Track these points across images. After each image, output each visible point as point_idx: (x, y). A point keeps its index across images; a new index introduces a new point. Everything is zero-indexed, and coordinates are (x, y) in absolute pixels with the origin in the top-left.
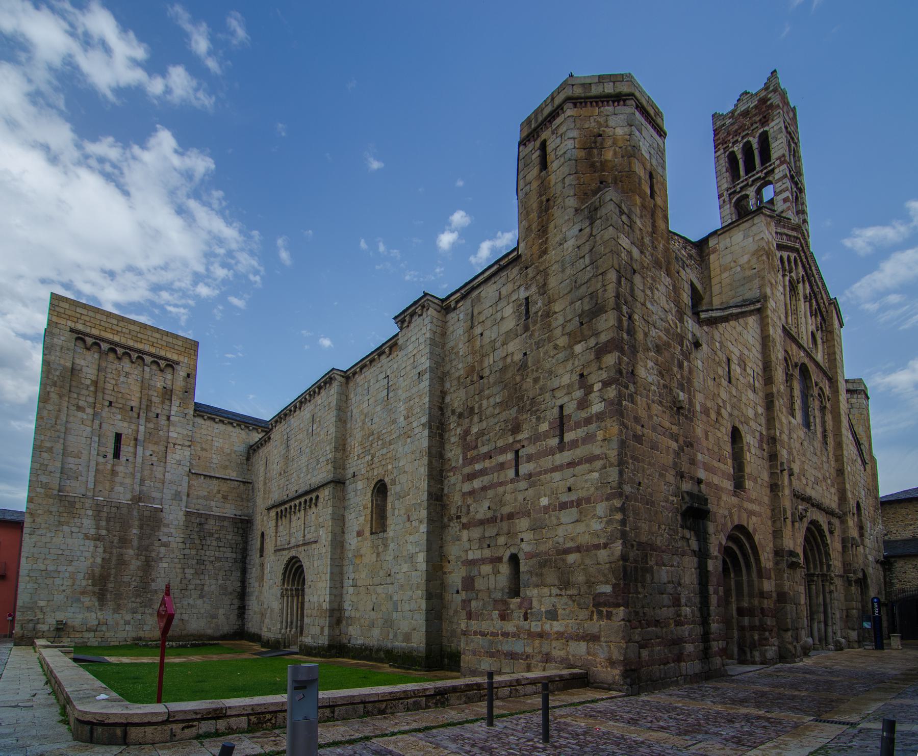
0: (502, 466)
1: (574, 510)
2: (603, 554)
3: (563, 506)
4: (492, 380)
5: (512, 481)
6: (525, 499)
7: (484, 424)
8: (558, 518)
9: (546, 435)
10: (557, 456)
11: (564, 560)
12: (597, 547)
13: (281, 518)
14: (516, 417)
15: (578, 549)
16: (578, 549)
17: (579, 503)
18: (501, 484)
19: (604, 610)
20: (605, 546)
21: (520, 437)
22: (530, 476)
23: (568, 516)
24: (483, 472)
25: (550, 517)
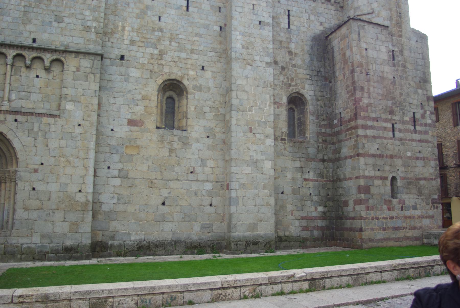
0: (385, 128)
1: (422, 161)
2: (434, 183)
3: (417, 158)
4: (375, 79)
5: (391, 139)
6: (399, 150)
7: (372, 101)
8: (416, 164)
9: (408, 123)
10: (414, 135)
11: (419, 183)
12: (432, 179)
14: (392, 107)
15: (425, 179)
16: (425, 179)
17: (424, 159)
18: (385, 138)
19: (435, 205)
20: (435, 180)
21: (394, 118)
22: (401, 139)
23: (420, 163)
24: (372, 127)
25: (412, 162)
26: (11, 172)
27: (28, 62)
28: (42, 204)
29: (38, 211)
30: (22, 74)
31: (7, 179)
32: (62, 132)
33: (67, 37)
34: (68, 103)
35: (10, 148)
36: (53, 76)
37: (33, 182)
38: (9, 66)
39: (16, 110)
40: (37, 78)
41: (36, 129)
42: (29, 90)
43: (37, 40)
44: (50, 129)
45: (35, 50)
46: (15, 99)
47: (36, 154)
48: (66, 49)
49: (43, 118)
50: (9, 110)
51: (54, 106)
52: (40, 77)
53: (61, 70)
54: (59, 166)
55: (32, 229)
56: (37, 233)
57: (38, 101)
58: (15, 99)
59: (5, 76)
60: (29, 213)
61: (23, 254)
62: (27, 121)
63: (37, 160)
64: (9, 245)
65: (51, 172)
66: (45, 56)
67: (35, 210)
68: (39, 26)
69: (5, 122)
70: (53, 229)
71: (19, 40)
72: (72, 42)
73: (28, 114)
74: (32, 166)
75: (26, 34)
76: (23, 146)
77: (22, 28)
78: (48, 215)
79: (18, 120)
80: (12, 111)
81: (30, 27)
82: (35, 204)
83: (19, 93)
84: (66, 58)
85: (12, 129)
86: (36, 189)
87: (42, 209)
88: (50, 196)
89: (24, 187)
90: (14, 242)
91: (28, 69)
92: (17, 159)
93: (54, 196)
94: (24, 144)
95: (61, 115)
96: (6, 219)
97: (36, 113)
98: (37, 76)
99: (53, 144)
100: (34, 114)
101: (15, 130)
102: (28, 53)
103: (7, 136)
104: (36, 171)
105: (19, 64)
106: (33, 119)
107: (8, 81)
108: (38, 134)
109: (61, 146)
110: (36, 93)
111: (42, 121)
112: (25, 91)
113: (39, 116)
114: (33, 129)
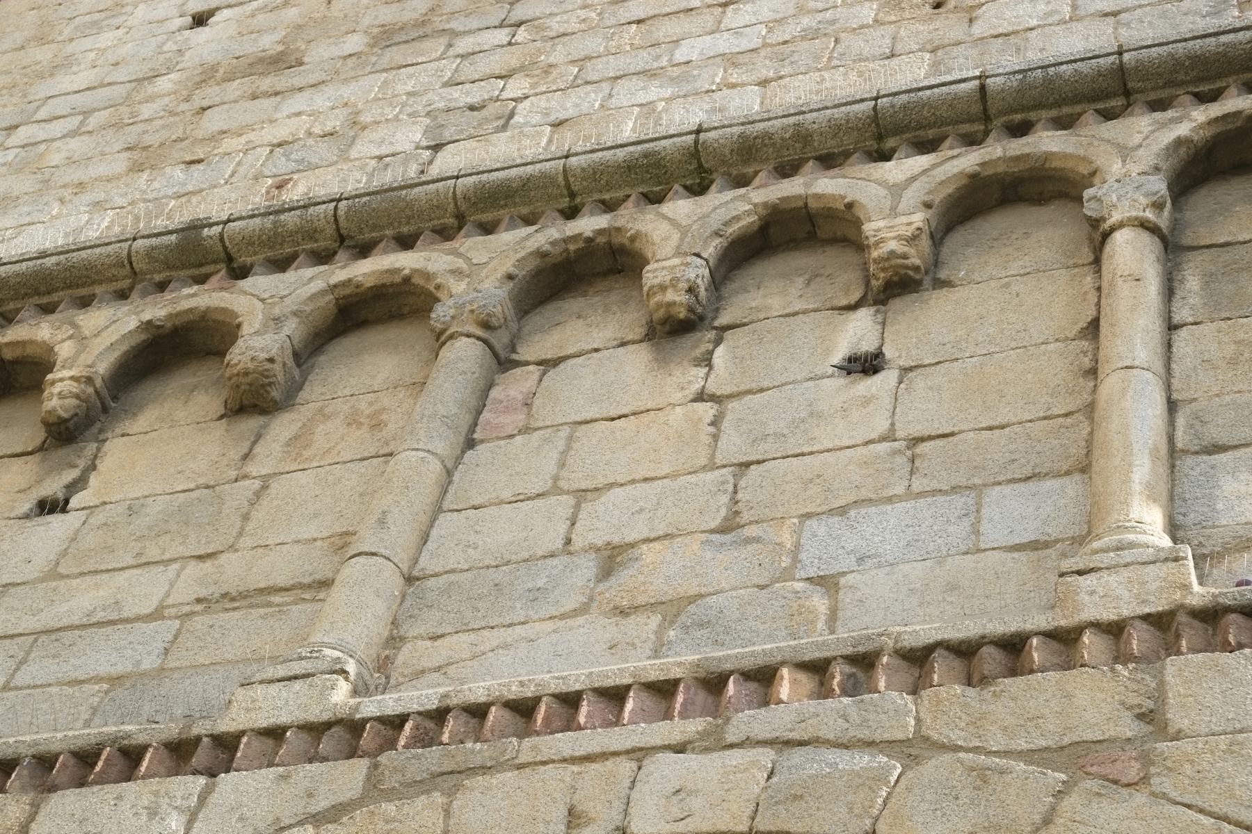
69: (1146, 760)
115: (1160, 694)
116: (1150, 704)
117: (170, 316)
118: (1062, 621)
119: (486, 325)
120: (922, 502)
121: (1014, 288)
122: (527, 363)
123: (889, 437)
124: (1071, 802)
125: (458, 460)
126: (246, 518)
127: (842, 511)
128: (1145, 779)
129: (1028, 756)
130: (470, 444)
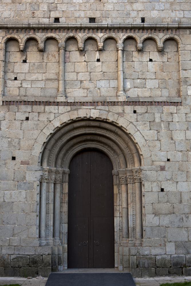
13: (23, 51)
26: (134, 171)
27: (140, 45)
28: (174, 208)
29: (169, 215)
30: (134, 60)
31: (129, 180)
32: (186, 121)
33: (177, 12)
34: (188, 87)
35: (130, 144)
36: (168, 58)
37: (161, 182)
38: (120, 51)
39: (134, 101)
40: (150, 62)
41: (157, 120)
42: (144, 77)
43: (146, 19)
44: (172, 118)
45: (146, 31)
46: (131, 88)
47: (161, 149)
48: (180, 26)
49: (164, 107)
50: (126, 100)
51: (174, 93)
52: (153, 60)
53: (176, 50)
54: (188, 161)
55: (165, 237)
56: (170, 242)
57: (154, 88)
58: (131, 88)
59: (116, 63)
60: (159, 219)
61: (158, 267)
62: (146, 112)
63: (163, 156)
64: (141, 256)
65: (179, 169)
66: (157, 36)
67: (166, 214)
68: (145, 3)
69: (123, 115)
70: (188, 236)
71: (128, 21)
72: (184, 17)
73: (147, 103)
74: (158, 163)
75: (133, 14)
76: (146, 140)
77: (128, 7)
78: (181, 221)
79: (137, 111)
80: (130, 102)
81: (138, 6)
82: (165, 207)
83: (133, 80)
84: (181, 36)
85: (131, 122)
86: (165, 190)
87: (174, 213)
88: (181, 198)
89: (152, 189)
90: (146, 253)
91: (140, 53)
92: (139, 156)
93: (185, 198)
94: (146, 139)
95: (184, 102)
96: (132, 226)
97: (155, 102)
98: (151, 60)
99: (179, 136)
100: (154, 103)
101: (135, 123)
102: (138, 34)
103: (127, 130)
104: (163, 169)
105: (131, 48)
106: (154, 109)
107: (120, 68)
108: (161, 127)
109: (187, 138)
110: (151, 79)
111: (163, 110)
112: (140, 78)
113: (158, 105)
114: (154, 121)
115: (124, 109)
116: (123, 110)
117: (29, 37)
118: (118, 101)
119: (64, 48)
120: (105, 80)
121: (111, 53)
122: (67, 51)
123: (102, 71)
124: (119, 118)
125: (65, 65)
126: (46, 68)
127: (99, 80)
128: (123, 116)
129: (116, 113)
130: (65, 63)
